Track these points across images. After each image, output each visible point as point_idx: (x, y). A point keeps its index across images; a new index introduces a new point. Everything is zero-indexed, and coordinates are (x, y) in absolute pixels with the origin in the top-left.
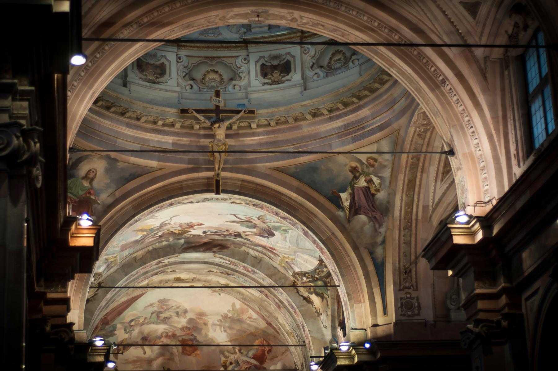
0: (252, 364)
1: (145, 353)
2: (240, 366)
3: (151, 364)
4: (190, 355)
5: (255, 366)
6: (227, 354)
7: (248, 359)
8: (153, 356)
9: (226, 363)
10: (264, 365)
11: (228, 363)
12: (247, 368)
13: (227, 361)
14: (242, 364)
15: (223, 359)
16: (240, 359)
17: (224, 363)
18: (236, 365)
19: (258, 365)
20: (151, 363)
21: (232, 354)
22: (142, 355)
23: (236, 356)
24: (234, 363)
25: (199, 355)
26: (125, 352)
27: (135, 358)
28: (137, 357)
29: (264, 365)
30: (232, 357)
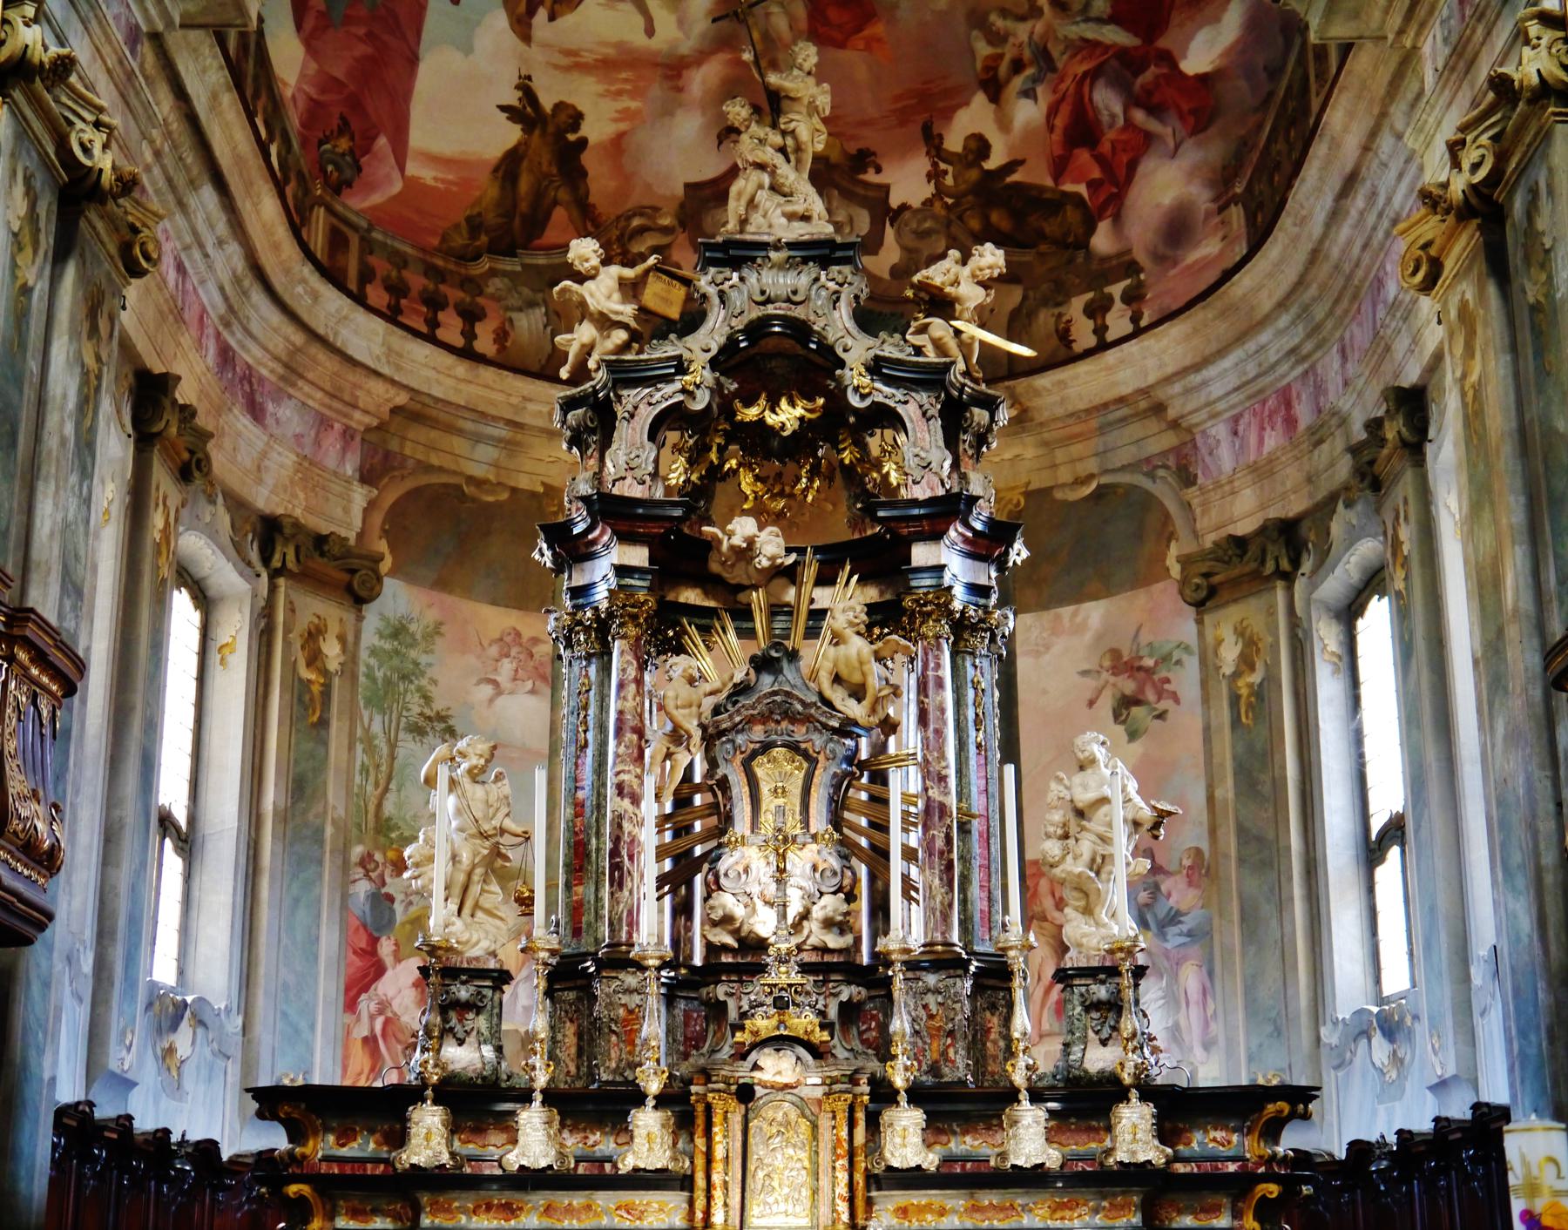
0: (1107, 48)
1: (650, 31)
2: (1053, 69)
3: (680, 83)
4: (842, 45)
5: (1122, 53)
6: (999, 23)
7: (1090, 32)
8: (686, 47)
9: (995, 69)
10: (1163, 43)
11: (1004, 68)
12: (1086, 74)
13: (1001, 57)
14: (1065, 57)
15: (983, 49)
16: (1056, 38)
17: (987, 68)
18: (1040, 70)
19: (1136, 48)
20: (679, 76)
21: (1022, 18)
22: (638, 39)
23: (1039, 27)
24: (1031, 64)
25: (879, 40)
26: (562, 15)
27: (611, 52)
28: (620, 46)
29: (1163, 43)
30: (1022, 31)
